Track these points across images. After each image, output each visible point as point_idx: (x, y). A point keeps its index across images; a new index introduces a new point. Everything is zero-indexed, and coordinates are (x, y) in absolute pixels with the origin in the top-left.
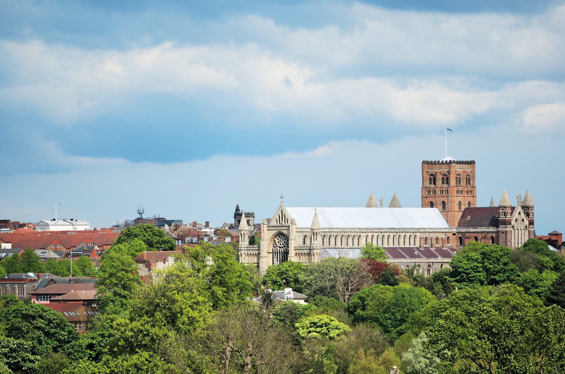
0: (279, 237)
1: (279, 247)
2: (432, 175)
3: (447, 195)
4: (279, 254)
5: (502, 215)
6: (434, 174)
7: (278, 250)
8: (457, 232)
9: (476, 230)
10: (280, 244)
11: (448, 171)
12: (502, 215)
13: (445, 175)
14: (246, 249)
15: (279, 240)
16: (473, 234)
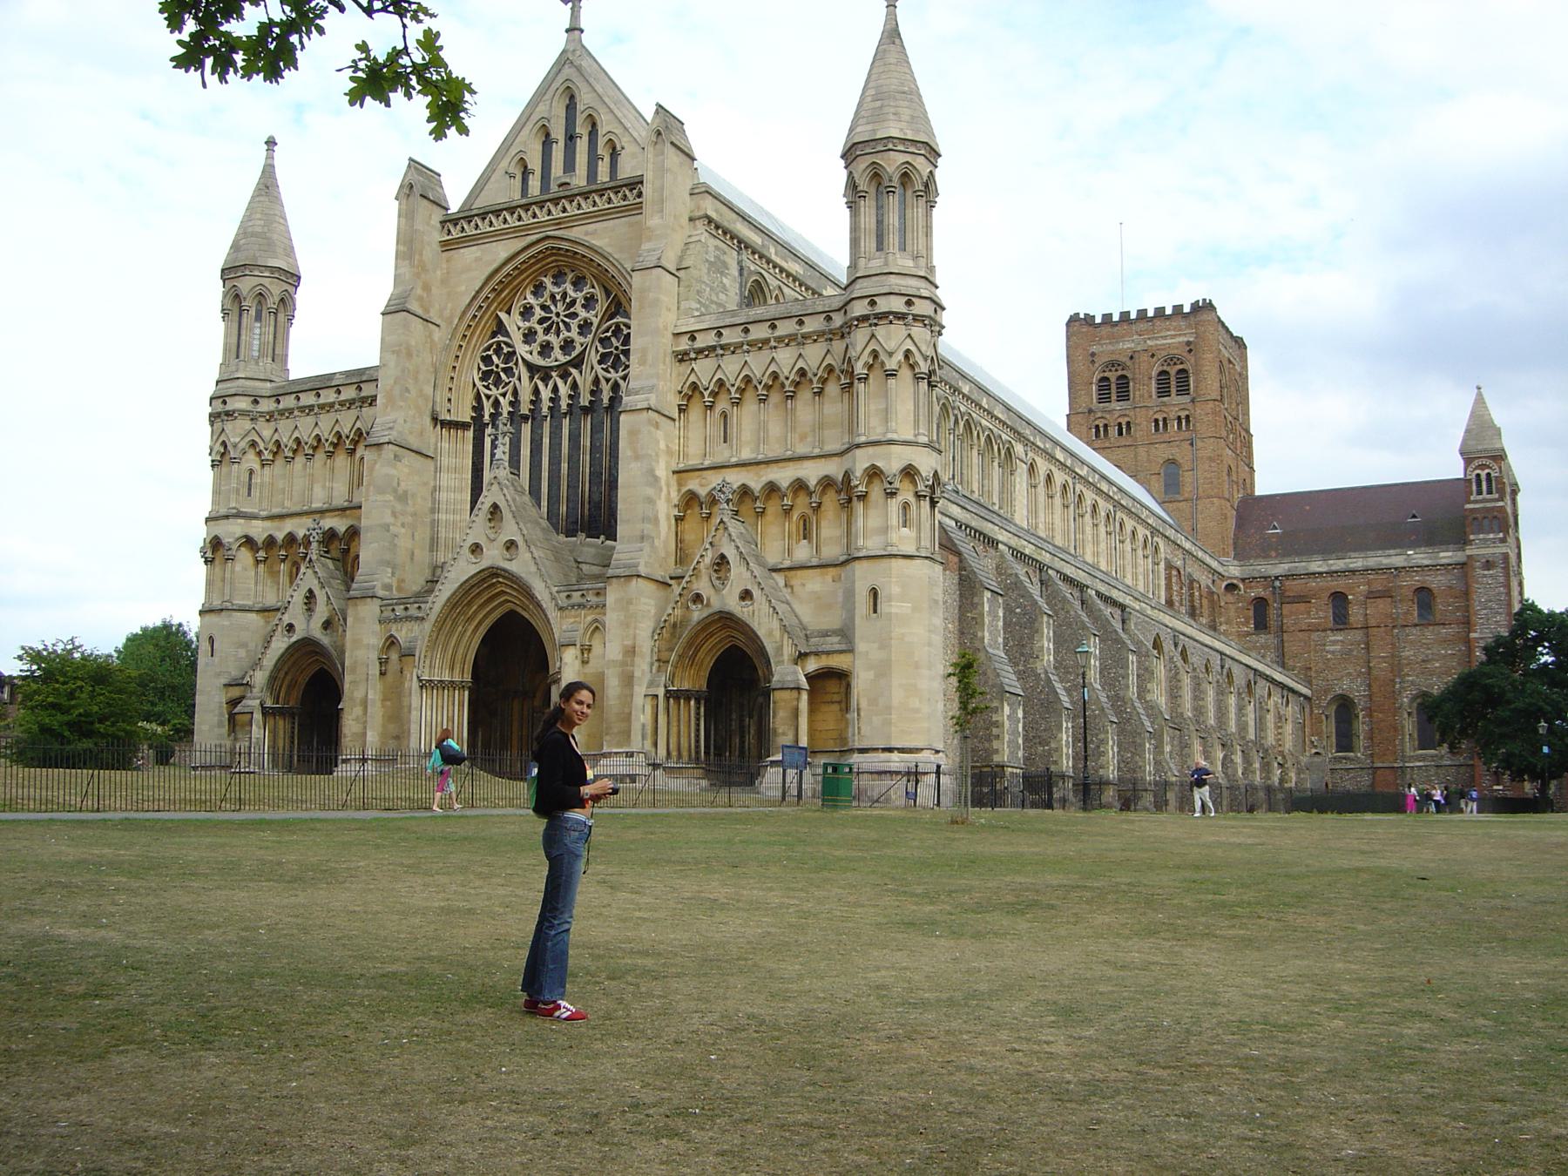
0: (538, 290)
1: (532, 369)
2: (1113, 364)
3: (1187, 435)
4: (526, 429)
5: (1480, 492)
6: (1125, 359)
7: (526, 396)
8: (1243, 580)
9: (1338, 565)
10: (546, 349)
11: (1188, 343)
12: (1480, 492)
13: (1171, 360)
14: (266, 406)
15: (539, 313)
16: (1321, 583)
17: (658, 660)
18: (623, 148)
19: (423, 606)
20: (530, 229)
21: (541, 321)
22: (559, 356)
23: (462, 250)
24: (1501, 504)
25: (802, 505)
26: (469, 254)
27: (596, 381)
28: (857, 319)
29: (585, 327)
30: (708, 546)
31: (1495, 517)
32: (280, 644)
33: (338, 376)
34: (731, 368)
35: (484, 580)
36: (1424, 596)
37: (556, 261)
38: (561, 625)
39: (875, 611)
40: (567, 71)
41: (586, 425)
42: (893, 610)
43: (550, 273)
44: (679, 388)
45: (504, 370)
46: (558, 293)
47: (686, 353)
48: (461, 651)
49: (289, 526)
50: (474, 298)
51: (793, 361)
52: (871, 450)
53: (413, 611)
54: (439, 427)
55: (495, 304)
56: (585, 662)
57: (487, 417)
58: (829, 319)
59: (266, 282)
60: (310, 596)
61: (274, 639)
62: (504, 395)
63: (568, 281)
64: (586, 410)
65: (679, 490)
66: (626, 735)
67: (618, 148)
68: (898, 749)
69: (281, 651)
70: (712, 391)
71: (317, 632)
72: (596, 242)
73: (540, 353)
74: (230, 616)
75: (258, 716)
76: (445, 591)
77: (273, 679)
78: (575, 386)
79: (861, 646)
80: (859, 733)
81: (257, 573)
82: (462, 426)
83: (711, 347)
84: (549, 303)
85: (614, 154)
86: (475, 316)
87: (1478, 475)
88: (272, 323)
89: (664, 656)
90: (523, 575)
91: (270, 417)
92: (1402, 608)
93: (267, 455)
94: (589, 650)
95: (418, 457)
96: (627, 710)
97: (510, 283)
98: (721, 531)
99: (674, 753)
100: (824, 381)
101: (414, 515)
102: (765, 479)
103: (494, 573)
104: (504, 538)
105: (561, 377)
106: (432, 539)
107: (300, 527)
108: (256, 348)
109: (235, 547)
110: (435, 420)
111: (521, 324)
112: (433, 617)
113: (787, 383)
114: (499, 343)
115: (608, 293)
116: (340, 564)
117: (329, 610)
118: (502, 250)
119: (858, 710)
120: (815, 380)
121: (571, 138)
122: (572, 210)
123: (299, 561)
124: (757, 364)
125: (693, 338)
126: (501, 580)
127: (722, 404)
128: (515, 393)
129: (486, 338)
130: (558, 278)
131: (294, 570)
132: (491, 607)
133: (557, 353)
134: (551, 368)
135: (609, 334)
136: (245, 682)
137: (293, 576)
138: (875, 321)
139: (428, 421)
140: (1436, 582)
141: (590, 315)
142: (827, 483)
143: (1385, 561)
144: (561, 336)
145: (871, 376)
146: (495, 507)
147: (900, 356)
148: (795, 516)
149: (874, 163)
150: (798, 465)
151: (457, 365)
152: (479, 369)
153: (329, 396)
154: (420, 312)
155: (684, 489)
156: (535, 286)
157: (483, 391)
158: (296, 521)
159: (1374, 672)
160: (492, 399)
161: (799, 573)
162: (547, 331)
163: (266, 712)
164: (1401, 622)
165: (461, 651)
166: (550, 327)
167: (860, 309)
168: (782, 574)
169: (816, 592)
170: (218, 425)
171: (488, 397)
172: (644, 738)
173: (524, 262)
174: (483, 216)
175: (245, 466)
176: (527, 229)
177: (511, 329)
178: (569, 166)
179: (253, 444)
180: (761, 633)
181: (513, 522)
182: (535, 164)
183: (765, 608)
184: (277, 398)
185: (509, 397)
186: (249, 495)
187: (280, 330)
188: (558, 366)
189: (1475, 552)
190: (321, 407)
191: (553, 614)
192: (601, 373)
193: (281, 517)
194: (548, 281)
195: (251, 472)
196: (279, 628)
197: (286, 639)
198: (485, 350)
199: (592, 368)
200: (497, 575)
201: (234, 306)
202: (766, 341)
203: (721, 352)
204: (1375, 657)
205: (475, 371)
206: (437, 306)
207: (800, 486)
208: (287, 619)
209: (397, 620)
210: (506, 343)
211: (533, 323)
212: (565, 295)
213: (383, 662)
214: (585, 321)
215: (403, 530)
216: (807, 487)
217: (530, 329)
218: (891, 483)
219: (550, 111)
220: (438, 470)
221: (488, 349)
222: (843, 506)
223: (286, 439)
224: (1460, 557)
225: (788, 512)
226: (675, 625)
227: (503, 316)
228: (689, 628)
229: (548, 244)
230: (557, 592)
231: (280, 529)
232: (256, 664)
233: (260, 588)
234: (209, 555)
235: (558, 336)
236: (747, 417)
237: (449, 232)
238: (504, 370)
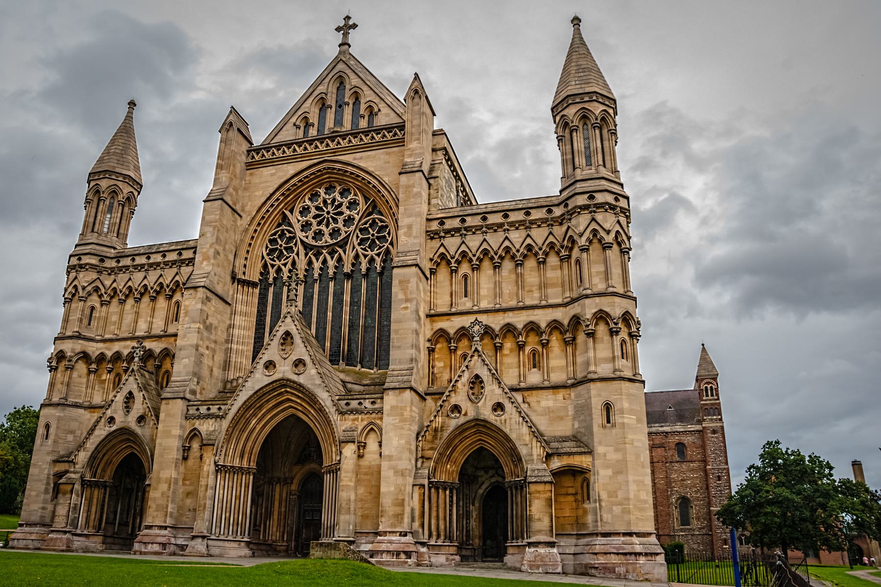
0: (314, 196)
5: (707, 396)
7: (302, 264)
10: (318, 235)
12: (707, 396)
15: (314, 211)
17: (422, 457)
18: (379, 110)
19: (223, 407)
20: (313, 156)
21: (315, 217)
22: (327, 239)
23: (261, 169)
24: (718, 401)
25: (532, 343)
26: (266, 172)
27: (357, 257)
28: (580, 207)
29: (349, 221)
30: (464, 368)
31: (716, 408)
32: (102, 432)
33: (164, 245)
34: (474, 242)
35: (274, 390)
36: (681, 447)
37: (329, 178)
38: (342, 425)
39: (608, 422)
40: (341, 66)
41: (348, 286)
42: (626, 421)
43: (325, 186)
44: (431, 257)
45: (286, 248)
46: (329, 199)
47: (436, 233)
48: (250, 444)
49: (117, 347)
50: (268, 199)
51: (521, 240)
52: (597, 299)
53: (214, 410)
54: (236, 283)
55: (283, 204)
56: (360, 456)
57: (271, 280)
58: (550, 211)
59: (120, 184)
60: (130, 396)
61: (97, 427)
62: (285, 265)
63: (337, 191)
64: (348, 276)
65: (432, 329)
66: (399, 517)
67: (376, 110)
68: (635, 533)
69: (103, 437)
70: (457, 260)
71: (133, 424)
72: (362, 164)
73: (313, 238)
74: (64, 410)
75: (77, 487)
76: (243, 396)
77: (93, 458)
78: (340, 259)
79: (600, 449)
80: (601, 520)
81: (88, 380)
82: (252, 284)
83: (456, 228)
84: (329, 202)
85: (372, 113)
86: (268, 211)
87: (706, 387)
88: (120, 211)
89: (429, 453)
90: (309, 386)
91: (112, 271)
92: (670, 453)
93: (106, 298)
94: (364, 447)
95: (221, 301)
96: (400, 497)
97: (295, 190)
98: (476, 358)
99: (434, 533)
100: (547, 254)
101: (215, 342)
102: (503, 322)
103: (284, 383)
104: (294, 357)
105: (329, 254)
106: (225, 361)
107: (125, 348)
108: (106, 226)
109: (74, 359)
110: (234, 278)
111: (300, 218)
112: (230, 416)
113: (518, 255)
114: (283, 231)
115: (366, 199)
116: (153, 377)
117: (144, 409)
118: (291, 169)
119: (600, 500)
120: (541, 252)
121: (340, 106)
122: (344, 143)
123: (122, 372)
124: (495, 240)
125: (442, 223)
126: (288, 389)
127: (465, 268)
128: (294, 263)
129: (274, 227)
130: (330, 189)
131: (117, 379)
132: (274, 413)
133: (327, 237)
134: (322, 247)
135: (367, 226)
136: (70, 459)
137: (117, 383)
138: (594, 209)
139: (228, 278)
140: (687, 440)
141: (354, 213)
142: (555, 325)
143: (661, 429)
144: (331, 227)
145: (590, 248)
146: (287, 334)
147: (613, 235)
148: (528, 349)
149: (584, 108)
150: (530, 312)
151: (253, 243)
152: (267, 247)
153: (158, 258)
154: (230, 203)
155: (435, 330)
156: (312, 195)
157: (269, 262)
158: (122, 343)
159: (658, 486)
160: (276, 267)
161: (534, 392)
162: (319, 223)
163: (84, 483)
164: (669, 460)
165: (250, 444)
166: (322, 220)
167: (582, 200)
168: (520, 393)
169: (549, 408)
170: (73, 275)
171: (273, 266)
172: (413, 520)
173: (307, 177)
174: (278, 147)
175: (89, 304)
176: (310, 156)
177: (293, 220)
178: (339, 121)
179: (97, 289)
180: (513, 436)
181: (302, 345)
182: (314, 118)
183: (516, 417)
184: (118, 258)
185: (289, 266)
186: (89, 324)
187: (124, 218)
188: (328, 246)
189: (707, 425)
190: (151, 265)
191: (334, 417)
192: (360, 251)
193: (111, 340)
194: (322, 191)
195: (93, 308)
196: (103, 420)
197: (107, 428)
198: (272, 235)
199: (354, 248)
200: (285, 386)
201: (95, 196)
202: (501, 225)
203: (465, 232)
204: (658, 478)
205: (264, 249)
206: (241, 204)
207: (532, 328)
208: (109, 413)
209: (199, 417)
210: (288, 231)
211: (309, 217)
212: (334, 200)
213: (186, 450)
214: (349, 216)
215: (207, 352)
216: (539, 327)
217: (307, 222)
218: (616, 324)
219: (327, 89)
220: (234, 313)
221: (275, 234)
222: (566, 343)
223: (120, 285)
224: (698, 427)
225: (521, 347)
226: (436, 430)
227: (287, 213)
228: (449, 432)
229: (325, 165)
230: (339, 400)
231: (109, 349)
232: (81, 446)
233: (89, 391)
234: (54, 364)
235: (327, 227)
236: (485, 279)
237: (253, 157)
238: (286, 248)
